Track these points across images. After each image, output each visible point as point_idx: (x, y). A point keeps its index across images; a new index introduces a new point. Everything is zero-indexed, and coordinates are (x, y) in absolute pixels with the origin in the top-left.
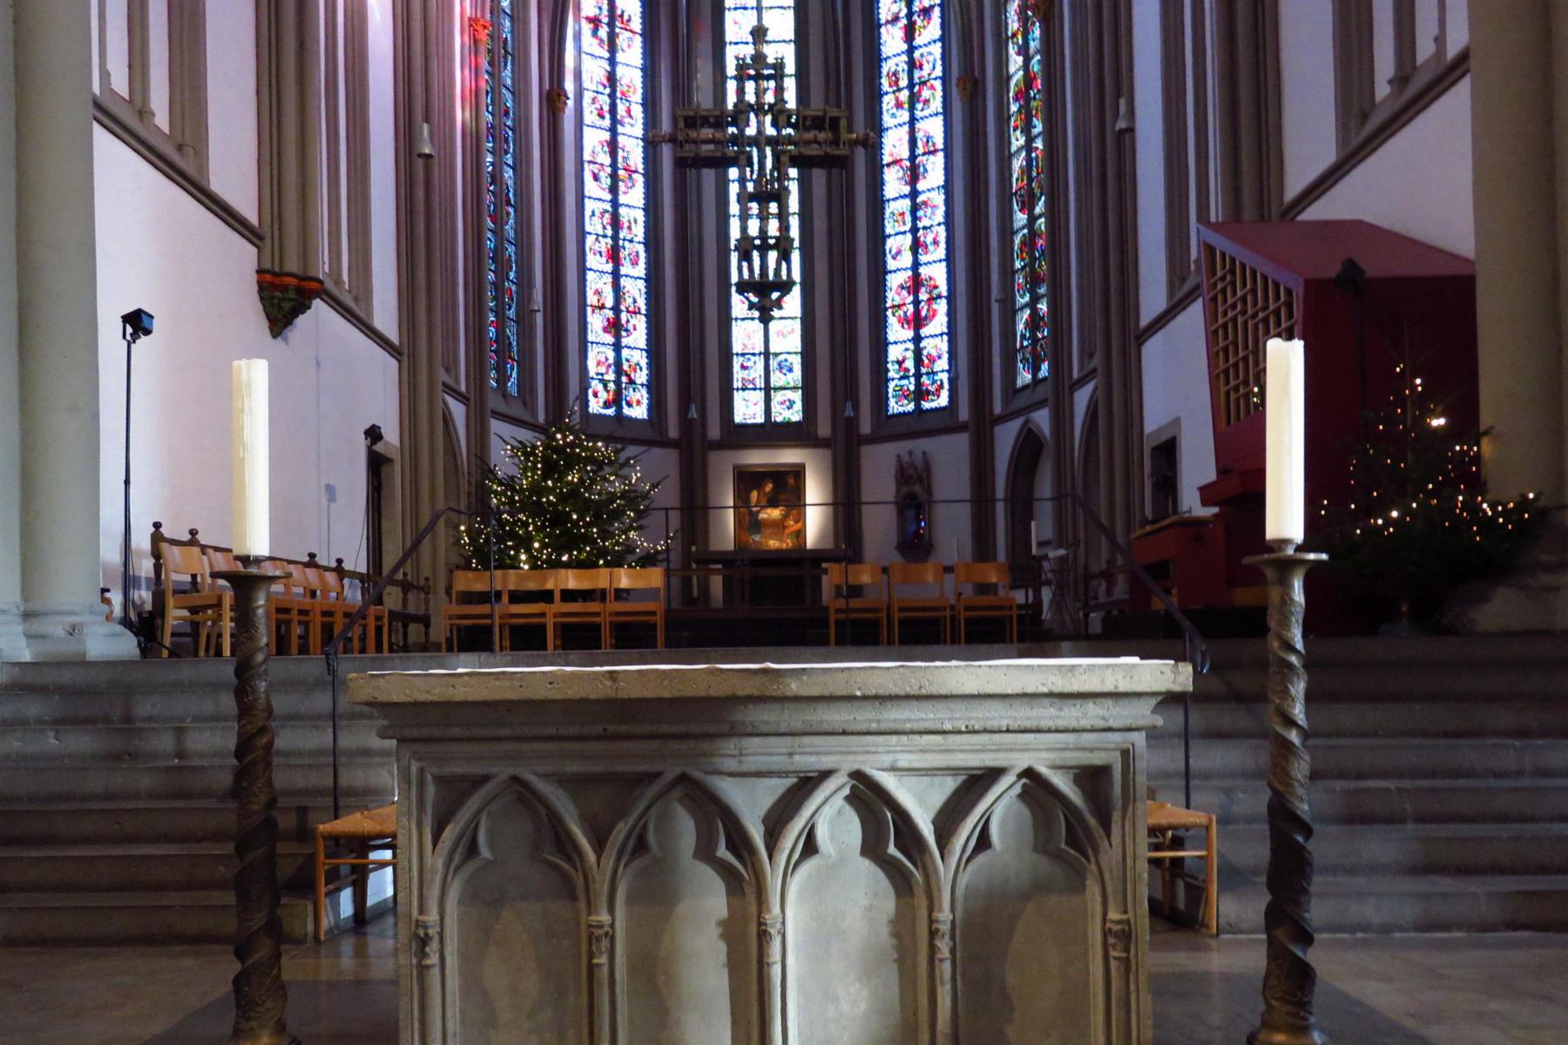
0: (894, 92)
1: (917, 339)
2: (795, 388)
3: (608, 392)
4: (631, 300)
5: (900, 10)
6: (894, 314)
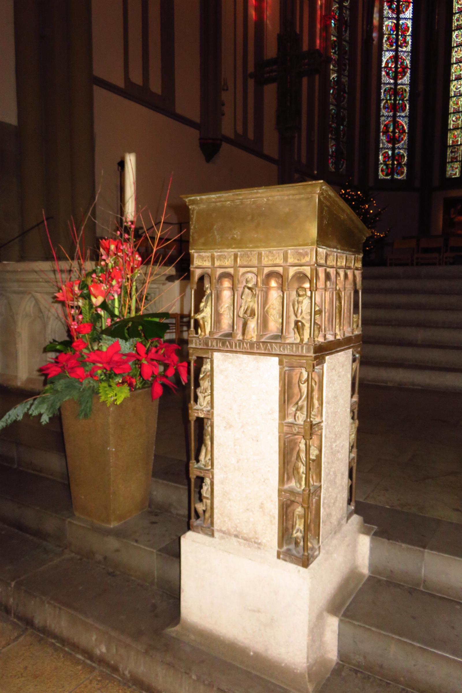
4: (401, 127)
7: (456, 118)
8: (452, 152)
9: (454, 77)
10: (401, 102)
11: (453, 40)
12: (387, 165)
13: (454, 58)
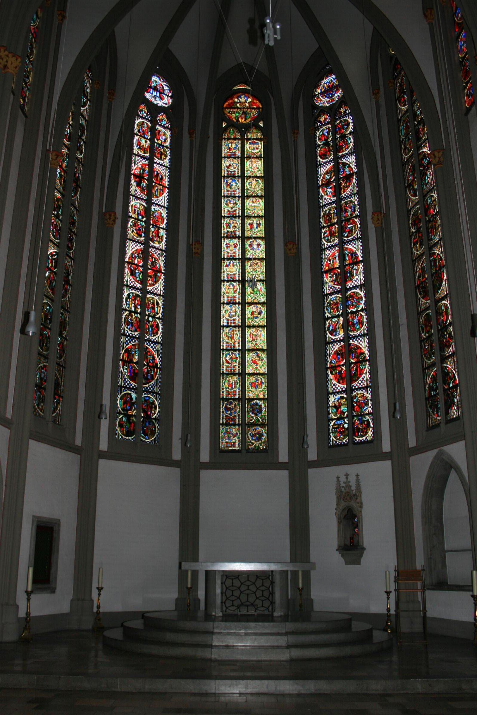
0: (328, 226)
1: (349, 390)
2: (262, 425)
3: (130, 424)
4: (151, 358)
5: (331, 178)
6: (332, 373)
7: (231, 358)
8: (227, 409)
9: (226, 299)
10: (151, 319)
11: (223, 249)
12: (129, 417)
13: (225, 274)
